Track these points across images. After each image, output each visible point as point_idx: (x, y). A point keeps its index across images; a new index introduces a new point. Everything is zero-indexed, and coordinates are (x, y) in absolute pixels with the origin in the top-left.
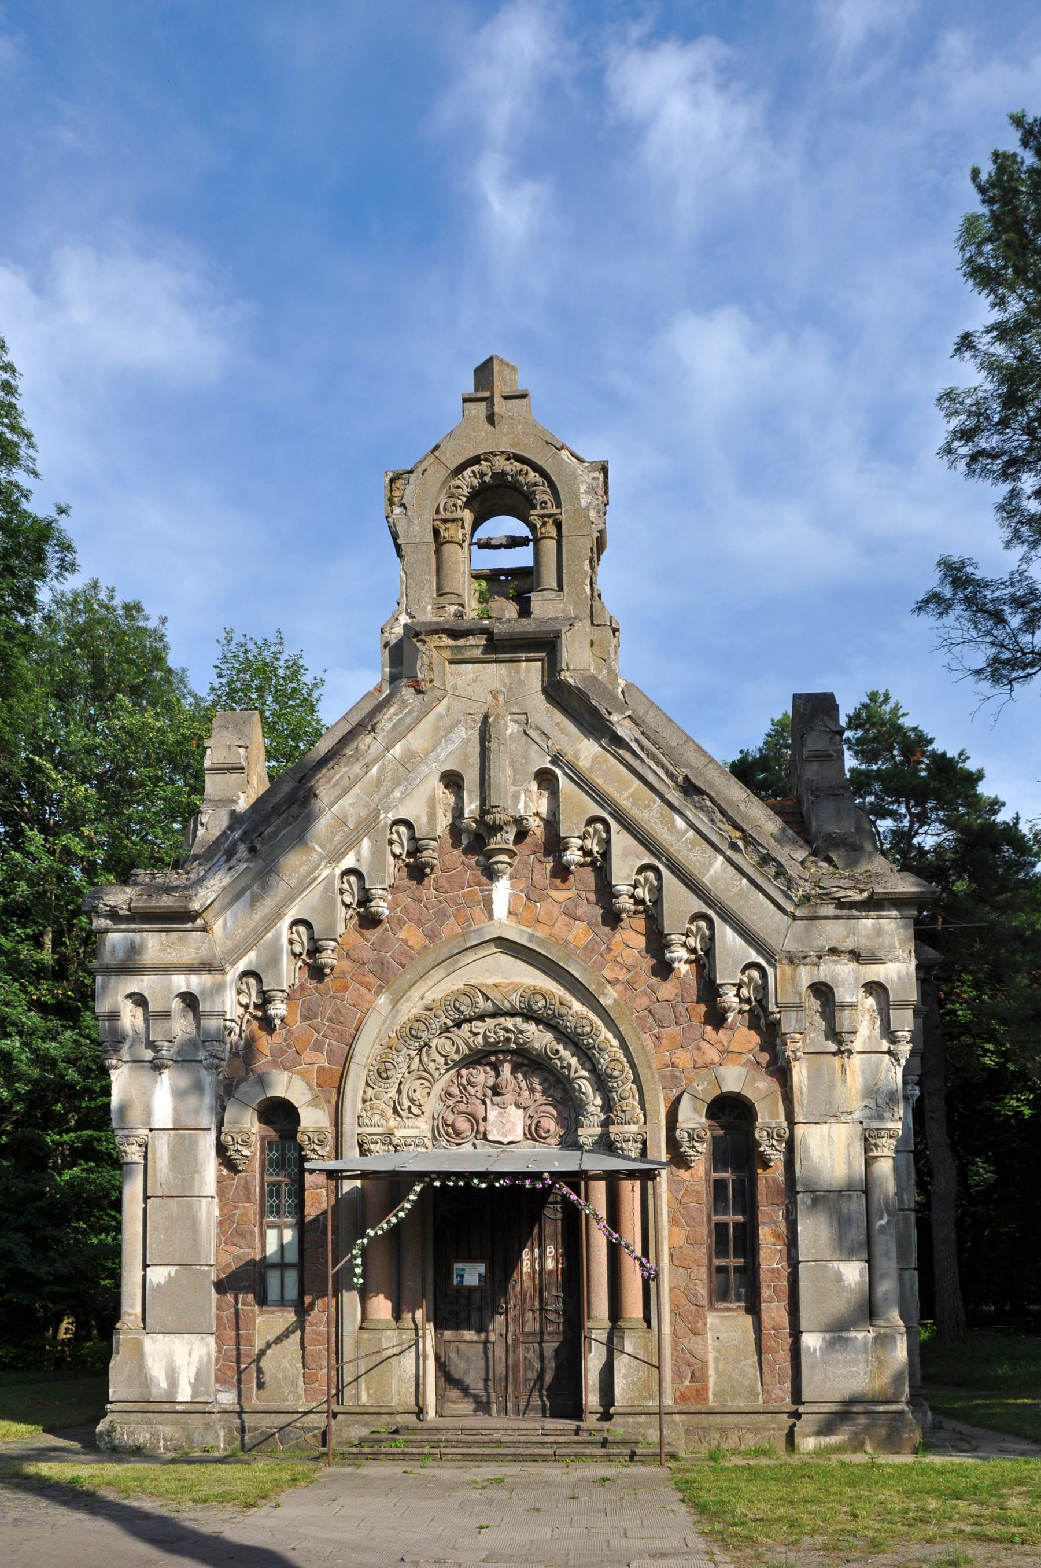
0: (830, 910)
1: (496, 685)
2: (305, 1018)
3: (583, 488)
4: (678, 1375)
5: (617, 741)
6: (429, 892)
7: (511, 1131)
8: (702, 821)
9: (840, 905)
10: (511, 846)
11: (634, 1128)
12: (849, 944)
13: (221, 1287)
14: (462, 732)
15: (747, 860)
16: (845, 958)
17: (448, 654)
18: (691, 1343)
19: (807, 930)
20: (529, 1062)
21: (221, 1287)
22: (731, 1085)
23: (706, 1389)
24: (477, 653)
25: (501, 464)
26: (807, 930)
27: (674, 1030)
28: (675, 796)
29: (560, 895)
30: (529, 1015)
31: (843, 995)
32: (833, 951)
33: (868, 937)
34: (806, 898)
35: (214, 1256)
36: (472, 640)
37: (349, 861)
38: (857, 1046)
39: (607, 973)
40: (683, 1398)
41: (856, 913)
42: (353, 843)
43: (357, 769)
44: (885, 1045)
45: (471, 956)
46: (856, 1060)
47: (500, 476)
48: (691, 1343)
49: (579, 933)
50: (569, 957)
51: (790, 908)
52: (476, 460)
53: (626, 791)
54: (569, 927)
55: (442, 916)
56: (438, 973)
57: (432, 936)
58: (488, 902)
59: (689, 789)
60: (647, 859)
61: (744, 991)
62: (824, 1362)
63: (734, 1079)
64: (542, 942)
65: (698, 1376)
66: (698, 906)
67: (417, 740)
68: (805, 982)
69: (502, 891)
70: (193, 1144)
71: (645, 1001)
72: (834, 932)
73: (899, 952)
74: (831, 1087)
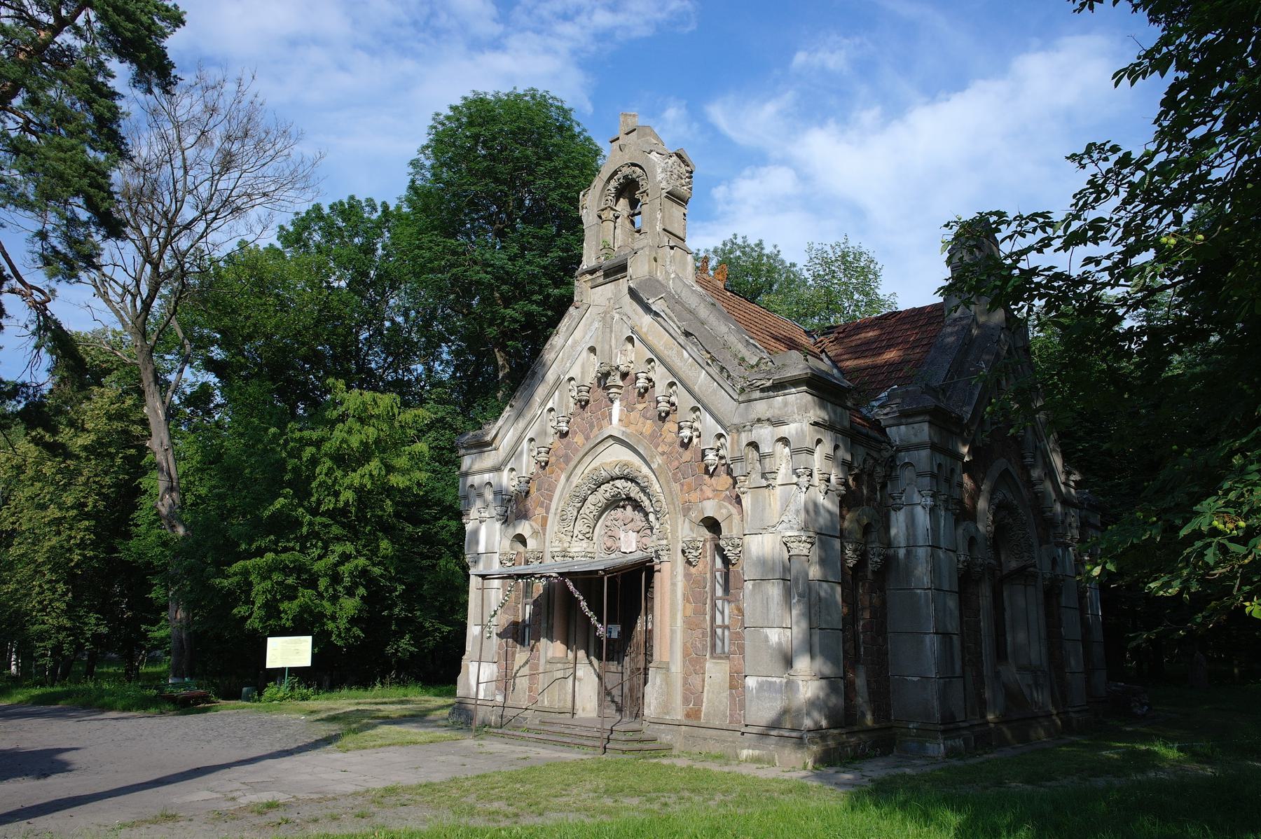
0: (757, 394)
1: (610, 295)
2: (538, 490)
3: (659, 171)
4: (686, 700)
5: (656, 314)
6: (587, 414)
7: (630, 545)
8: (694, 350)
9: (762, 390)
10: (621, 383)
11: (665, 542)
12: (768, 415)
13: (499, 635)
14: (596, 325)
15: (714, 370)
16: (766, 424)
17: (589, 284)
18: (695, 680)
19: (746, 409)
20: (615, 503)
21: (499, 635)
22: (709, 513)
23: (699, 711)
24: (601, 280)
25: (626, 171)
26: (746, 409)
27: (691, 479)
28: (682, 339)
29: (640, 407)
30: (626, 478)
31: (765, 449)
32: (759, 420)
33: (780, 409)
34: (742, 390)
35: (503, 620)
36: (598, 274)
37: (550, 405)
38: (779, 481)
39: (660, 449)
40: (688, 716)
41: (771, 394)
42: (550, 395)
43: (552, 356)
44: (795, 479)
45: (601, 448)
46: (778, 490)
47: (625, 177)
48: (695, 680)
49: (649, 427)
50: (639, 442)
51: (736, 397)
52: (615, 173)
53: (661, 340)
54: (644, 424)
55: (592, 426)
56: (588, 459)
57: (587, 438)
58: (610, 415)
59: (687, 334)
60: (672, 379)
61: (721, 452)
62: (758, 698)
63: (710, 509)
64: (628, 435)
65: (699, 702)
66: (694, 403)
67: (578, 334)
68: (744, 443)
69: (617, 408)
70: (491, 560)
71: (676, 463)
72: (762, 408)
73: (796, 416)
74: (763, 510)
